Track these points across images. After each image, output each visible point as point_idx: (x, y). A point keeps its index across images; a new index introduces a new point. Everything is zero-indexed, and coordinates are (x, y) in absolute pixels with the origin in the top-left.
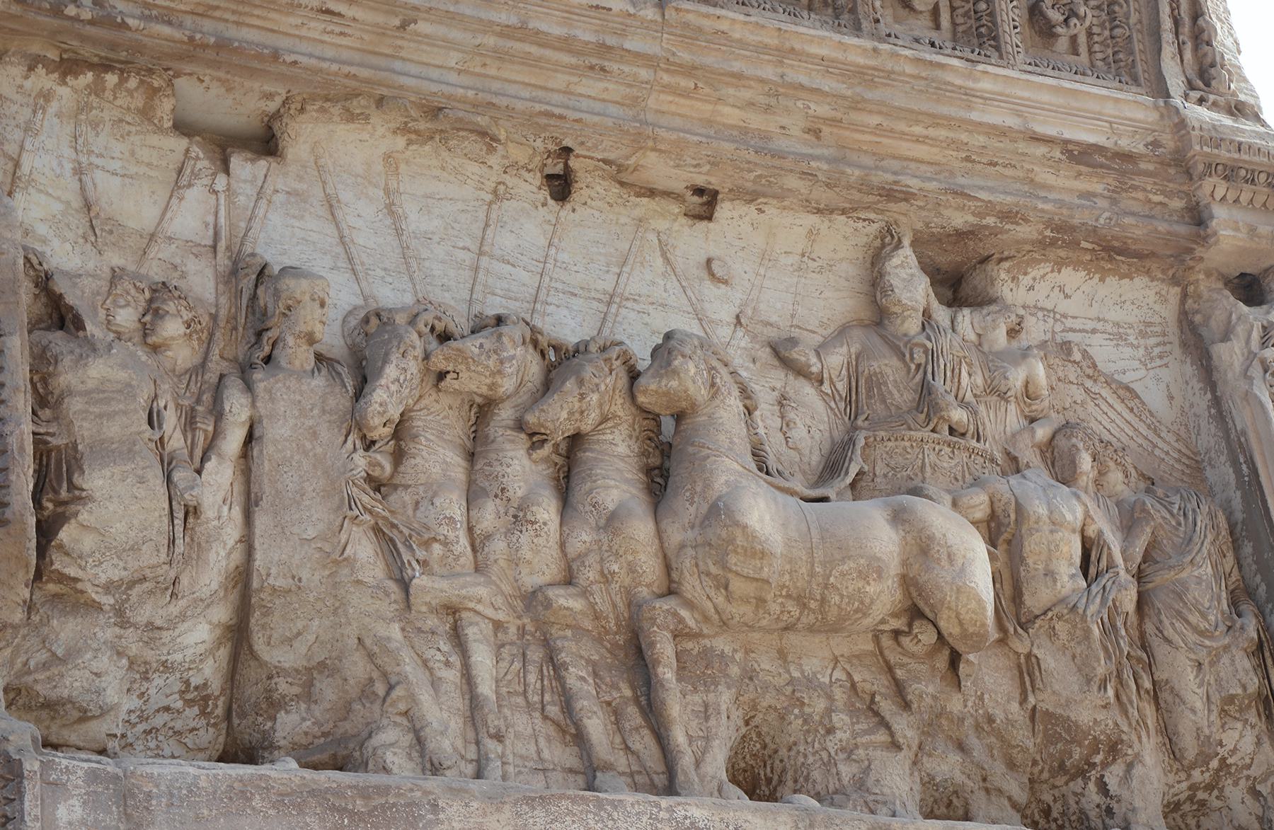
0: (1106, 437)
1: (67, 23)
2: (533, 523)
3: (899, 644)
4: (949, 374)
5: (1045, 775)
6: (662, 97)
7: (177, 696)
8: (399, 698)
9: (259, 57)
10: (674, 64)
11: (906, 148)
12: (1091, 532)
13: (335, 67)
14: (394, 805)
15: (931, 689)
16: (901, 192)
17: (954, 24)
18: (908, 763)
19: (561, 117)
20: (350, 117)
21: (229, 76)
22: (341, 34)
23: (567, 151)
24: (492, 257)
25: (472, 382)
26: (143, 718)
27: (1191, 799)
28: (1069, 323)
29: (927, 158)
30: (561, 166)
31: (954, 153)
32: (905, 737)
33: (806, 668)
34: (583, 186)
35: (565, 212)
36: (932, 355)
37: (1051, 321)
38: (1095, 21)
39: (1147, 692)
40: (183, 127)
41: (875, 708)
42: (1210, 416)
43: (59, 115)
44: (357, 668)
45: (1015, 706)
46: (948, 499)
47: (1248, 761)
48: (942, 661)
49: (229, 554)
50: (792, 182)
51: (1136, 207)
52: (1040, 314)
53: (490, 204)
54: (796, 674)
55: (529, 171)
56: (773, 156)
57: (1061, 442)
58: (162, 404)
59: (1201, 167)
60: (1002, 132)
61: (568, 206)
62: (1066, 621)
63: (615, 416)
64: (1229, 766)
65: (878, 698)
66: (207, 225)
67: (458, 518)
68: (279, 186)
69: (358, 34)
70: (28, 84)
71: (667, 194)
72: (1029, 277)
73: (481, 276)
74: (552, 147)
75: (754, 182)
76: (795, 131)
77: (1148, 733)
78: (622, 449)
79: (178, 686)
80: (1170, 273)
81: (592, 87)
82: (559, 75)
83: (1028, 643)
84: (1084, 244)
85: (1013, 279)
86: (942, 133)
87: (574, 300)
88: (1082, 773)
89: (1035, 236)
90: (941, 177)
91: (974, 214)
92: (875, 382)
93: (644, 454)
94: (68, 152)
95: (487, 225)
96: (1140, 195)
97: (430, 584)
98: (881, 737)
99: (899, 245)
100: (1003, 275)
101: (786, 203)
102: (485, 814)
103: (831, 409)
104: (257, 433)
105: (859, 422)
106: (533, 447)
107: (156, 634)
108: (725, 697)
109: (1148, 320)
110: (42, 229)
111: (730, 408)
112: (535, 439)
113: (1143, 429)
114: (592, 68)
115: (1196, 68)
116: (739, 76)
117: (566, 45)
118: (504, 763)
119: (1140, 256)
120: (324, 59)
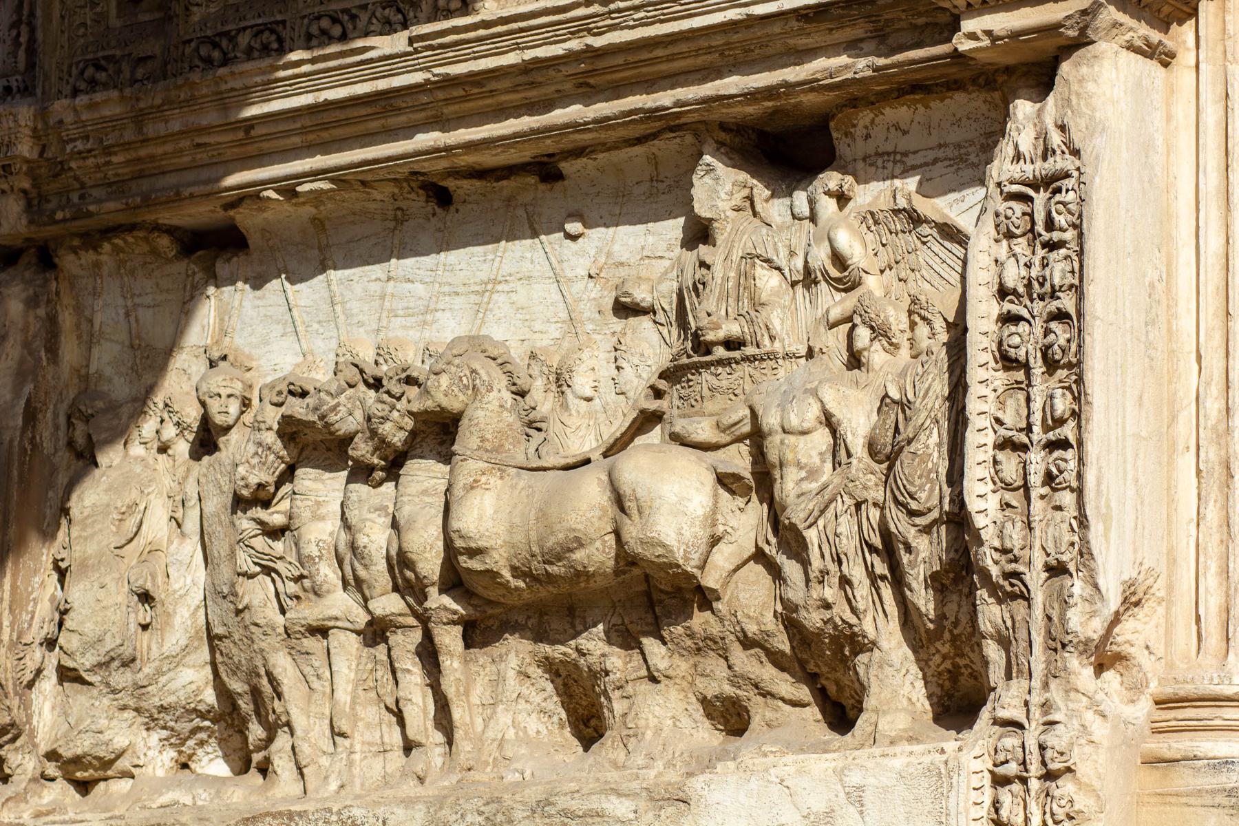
1: (62, 225)
11: (664, 67)
24: (396, 280)
35: (451, 216)
37: (890, 165)
39: (883, 578)
43: (110, 276)
47: (969, 630)
52: (880, 162)
61: (452, 209)
64: (959, 635)
70: (83, 261)
73: (387, 304)
85: (846, 135)
94: (120, 301)
107: (143, 690)
110: (108, 371)
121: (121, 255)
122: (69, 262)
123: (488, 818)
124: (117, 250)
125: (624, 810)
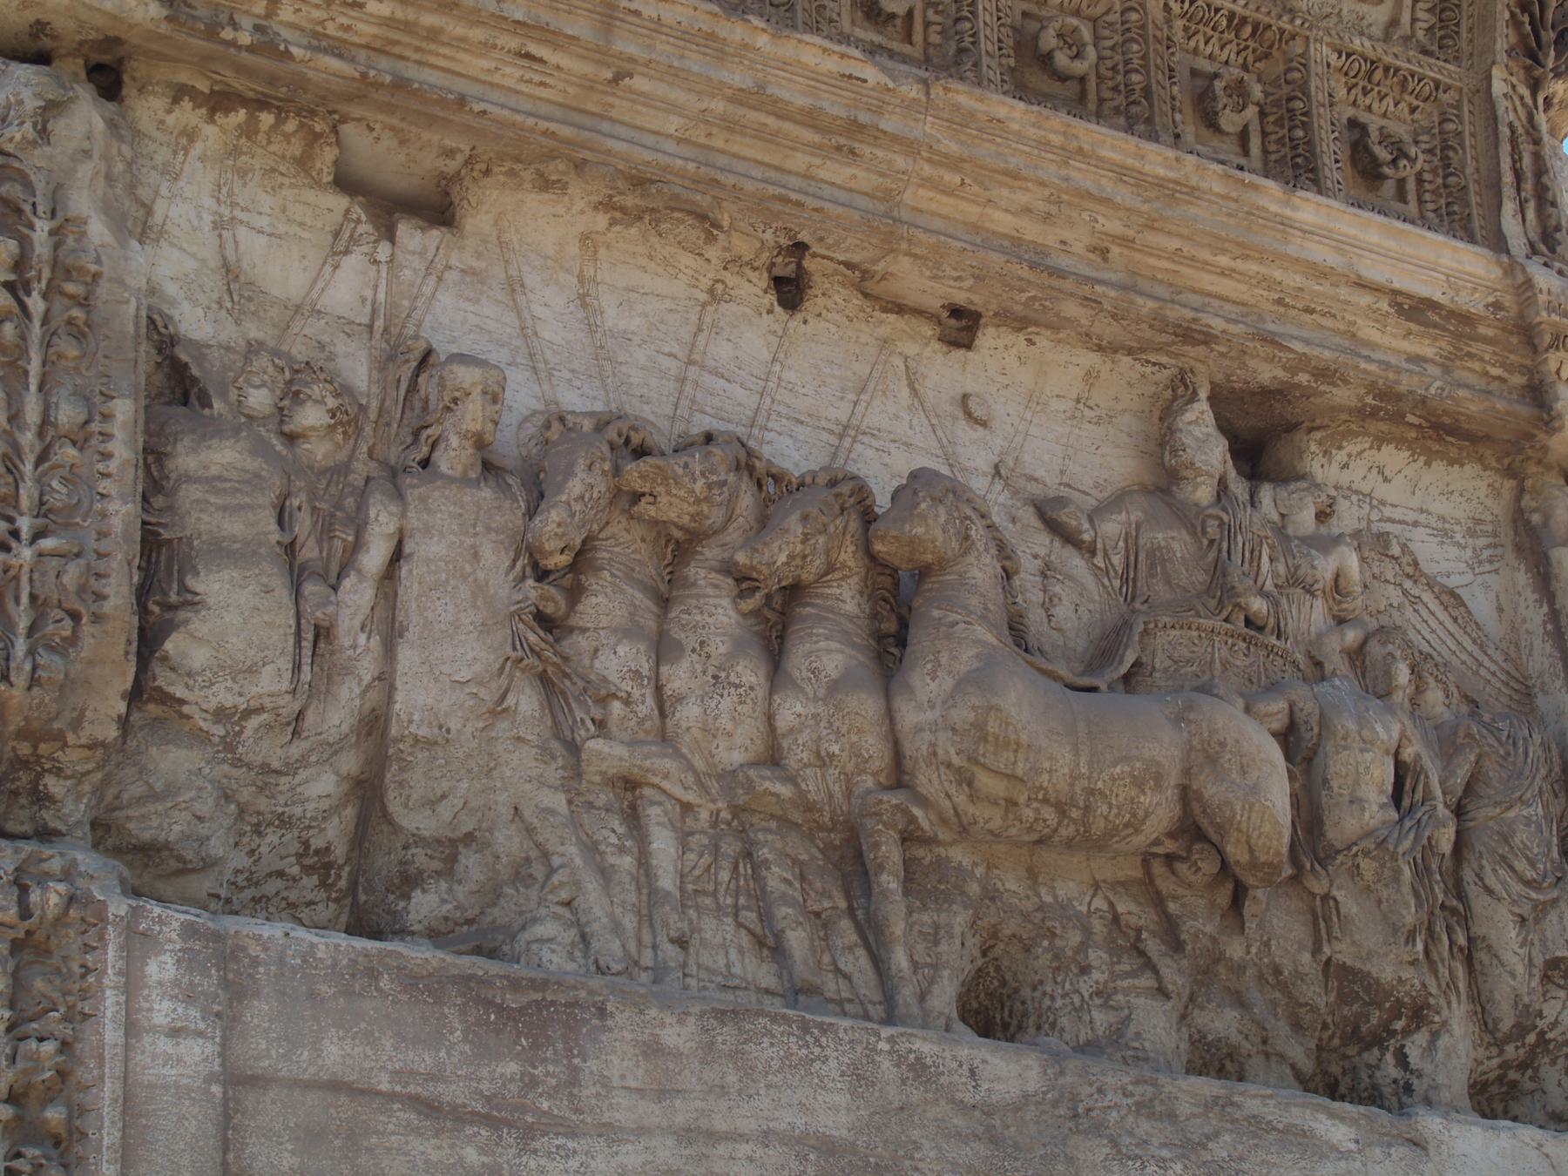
0: (1426, 648)
1: (220, 48)
2: (737, 686)
3: (1174, 872)
4: (1247, 555)
5: (1336, 1042)
6: (921, 192)
7: (293, 860)
8: (562, 884)
9: (442, 102)
10: (938, 153)
11: (1208, 282)
12: (1408, 754)
13: (530, 121)
14: (553, 1003)
15: (1210, 928)
16: (1200, 332)
17: (1265, 152)
18: (1175, 1017)
19: (799, 204)
20: (545, 184)
21: (404, 125)
22: (542, 84)
23: (800, 248)
24: (702, 367)
25: (673, 508)
26: (252, 882)
27: (1500, 1079)
28: (1388, 511)
29: (1233, 295)
30: (793, 266)
31: (1265, 293)
32: (1175, 983)
33: (1061, 893)
34: (819, 293)
35: (795, 324)
36: (1229, 531)
37: (1366, 506)
38: (1427, 167)
39: (1461, 949)
40: (345, 183)
41: (1141, 946)
42: (1546, 633)
43: (202, 159)
44: (508, 842)
45: (1306, 957)
46: (1240, 703)
48: (1224, 896)
49: (364, 692)
50: (1071, 309)
51: (1472, 379)
52: (1355, 498)
53: (704, 305)
54: (1048, 899)
55: (755, 269)
56: (1050, 275)
57: (1375, 649)
58: (296, 503)
59: (1547, 339)
60: (1321, 273)
61: (799, 316)
62: (1373, 858)
63: (844, 566)
64: (1550, 1041)
65: (1144, 935)
66: (364, 300)
67: (645, 672)
68: (454, 262)
69: (561, 85)
70: (170, 120)
71: (919, 312)
72: (1343, 453)
73: (688, 388)
74: (785, 242)
75: (1025, 304)
76: (1078, 248)
77: (1458, 996)
78: (850, 606)
79: (295, 847)
80: (1506, 461)
81: (836, 172)
82: (798, 155)
83: (1325, 882)
84: (1410, 418)
85: (1325, 453)
86: (1252, 267)
87: (800, 429)
88: (1378, 1040)
89: (1354, 402)
90: (1248, 320)
91: (1284, 368)
92: (1158, 557)
93: (874, 616)
94: (208, 202)
95: (700, 330)
96: (1477, 366)
97: (606, 749)
98: (1147, 981)
99: (1193, 398)
100: (1313, 447)
101: (1062, 335)
102: (663, 1025)
103: (1104, 586)
104: (408, 547)
105: (1137, 605)
106: (741, 595)
108: (960, 919)
109: (1478, 516)
110: (171, 289)
111: (981, 570)
112: (744, 586)
113: (1467, 643)
114: (839, 148)
115: (1539, 230)
116: (1014, 175)
117: (810, 118)
118: (685, 975)
119: (1474, 439)
120: (518, 112)
121: (243, 140)
122: (148, 109)
123: (1137, 1104)
124: (249, 130)
125: (1340, 1137)
